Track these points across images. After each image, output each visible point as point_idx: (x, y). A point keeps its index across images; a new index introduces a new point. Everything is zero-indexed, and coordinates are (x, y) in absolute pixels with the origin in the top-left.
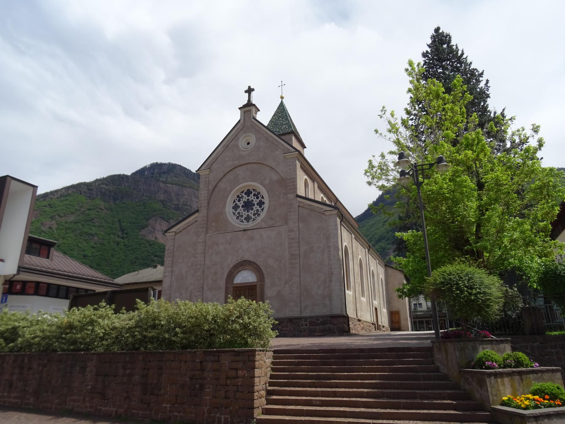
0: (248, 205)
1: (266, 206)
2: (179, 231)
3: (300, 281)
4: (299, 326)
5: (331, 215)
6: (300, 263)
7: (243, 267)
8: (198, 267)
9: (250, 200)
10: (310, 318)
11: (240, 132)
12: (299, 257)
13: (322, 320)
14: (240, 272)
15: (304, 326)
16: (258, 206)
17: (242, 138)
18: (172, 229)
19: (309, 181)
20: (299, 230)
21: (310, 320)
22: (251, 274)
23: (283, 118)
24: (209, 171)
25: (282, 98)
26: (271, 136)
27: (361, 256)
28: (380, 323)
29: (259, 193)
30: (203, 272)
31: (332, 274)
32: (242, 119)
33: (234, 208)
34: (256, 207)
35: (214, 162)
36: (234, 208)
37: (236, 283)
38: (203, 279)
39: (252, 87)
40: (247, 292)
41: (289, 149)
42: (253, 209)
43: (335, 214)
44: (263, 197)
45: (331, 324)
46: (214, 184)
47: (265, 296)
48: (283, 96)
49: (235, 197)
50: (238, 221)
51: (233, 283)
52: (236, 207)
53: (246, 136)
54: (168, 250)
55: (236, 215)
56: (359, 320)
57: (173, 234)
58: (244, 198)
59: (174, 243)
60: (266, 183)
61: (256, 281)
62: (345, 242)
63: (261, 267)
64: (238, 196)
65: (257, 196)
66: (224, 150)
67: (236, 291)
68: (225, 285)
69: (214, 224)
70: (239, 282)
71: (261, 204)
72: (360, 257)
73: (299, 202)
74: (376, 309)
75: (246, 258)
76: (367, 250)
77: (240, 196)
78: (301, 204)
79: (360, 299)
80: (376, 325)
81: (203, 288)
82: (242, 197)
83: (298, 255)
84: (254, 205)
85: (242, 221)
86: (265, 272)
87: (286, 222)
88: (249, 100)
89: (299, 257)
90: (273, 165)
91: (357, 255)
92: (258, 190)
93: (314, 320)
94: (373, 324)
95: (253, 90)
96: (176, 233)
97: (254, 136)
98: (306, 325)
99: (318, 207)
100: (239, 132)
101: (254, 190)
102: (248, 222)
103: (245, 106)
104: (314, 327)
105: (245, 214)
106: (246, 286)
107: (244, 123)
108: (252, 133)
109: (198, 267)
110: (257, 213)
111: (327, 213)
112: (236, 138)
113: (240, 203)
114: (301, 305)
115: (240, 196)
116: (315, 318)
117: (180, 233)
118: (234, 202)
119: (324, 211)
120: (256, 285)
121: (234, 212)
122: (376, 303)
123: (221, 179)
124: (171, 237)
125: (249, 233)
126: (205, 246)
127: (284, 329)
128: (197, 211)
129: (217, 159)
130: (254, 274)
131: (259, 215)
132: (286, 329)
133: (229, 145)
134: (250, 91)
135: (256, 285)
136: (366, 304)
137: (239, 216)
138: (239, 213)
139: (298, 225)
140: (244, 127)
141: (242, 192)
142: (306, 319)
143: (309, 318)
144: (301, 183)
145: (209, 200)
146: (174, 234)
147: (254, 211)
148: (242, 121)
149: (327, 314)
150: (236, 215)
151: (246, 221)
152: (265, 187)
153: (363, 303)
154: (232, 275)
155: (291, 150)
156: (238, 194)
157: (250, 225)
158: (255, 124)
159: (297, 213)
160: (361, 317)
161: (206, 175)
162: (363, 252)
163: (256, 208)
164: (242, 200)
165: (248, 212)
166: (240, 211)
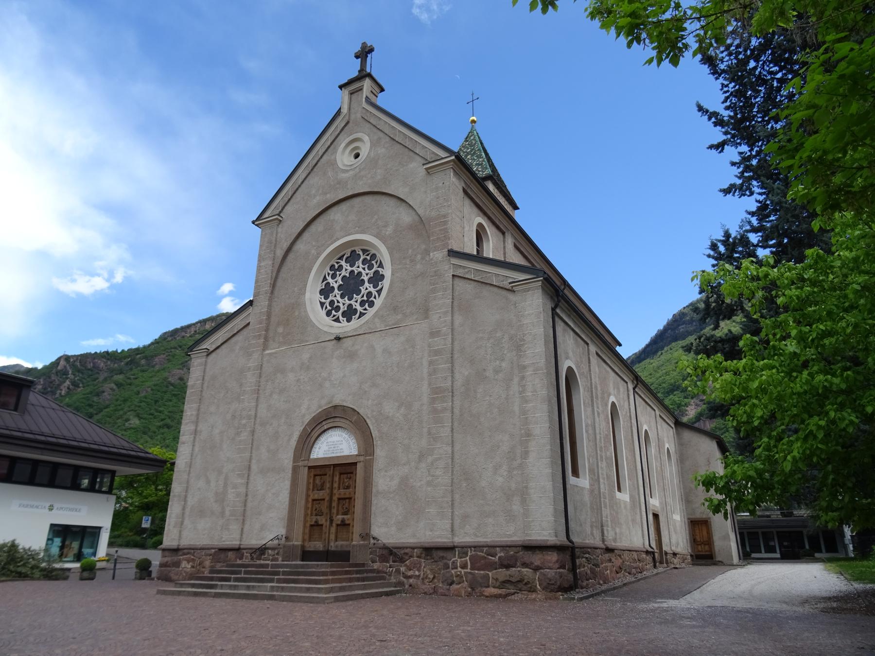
0: (351, 285)
1: (386, 284)
3: (453, 452)
4: (446, 567)
6: (452, 408)
7: (332, 420)
8: (244, 422)
9: (356, 272)
10: (475, 547)
11: (341, 135)
12: (453, 396)
13: (502, 554)
14: (325, 431)
15: (459, 569)
16: (371, 285)
18: (202, 343)
19: (490, 230)
20: (452, 330)
21: (473, 553)
22: (347, 436)
23: (472, 155)
24: (277, 219)
26: (400, 131)
27: (616, 398)
28: (665, 548)
29: (374, 256)
30: (253, 432)
31: (529, 434)
33: (322, 292)
34: (367, 287)
35: (289, 200)
36: (322, 292)
37: (315, 457)
38: (252, 448)
40: (337, 479)
41: (438, 155)
42: (360, 291)
44: (381, 265)
45: (525, 565)
46: (286, 245)
47: (374, 490)
50: (328, 320)
51: (308, 459)
52: (326, 291)
54: (193, 386)
55: (326, 308)
56: (609, 550)
59: (204, 372)
60: (387, 233)
62: (567, 358)
63: (368, 421)
64: (332, 267)
66: (309, 173)
67: (315, 476)
69: (280, 330)
70: (321, 455)
71: (377, 279)
72: (612, 399)
74: (656, 516)
75: (337, 401)
76: (631, 386)
77: (337, 266)
78: (460, 272)
79: (612, 497)
80: (656, 555)
81: (249, 468)
83: (450, 390)
85: (337, 320)
86: (375, 433)
87: (426, 313)
88: (362, 70)
89: (453, 396)
91: (603, 393)
92: (373, 251)
93: (483, 554)
94: (647, 552)
95: (371, 50)
96: (209, 353)
97: (367, 137)
98: (464, 566)
100: (339, 134)
101: (364, 251)
102: (349, 320)
104: (482, 572)
105: (344, 304)
106: (335, 466)
107: (349, 115)
108: (363, 132)
109: (244, 422)
110: (367, 301)
112: (332, 146)
113: (336, 282)
114: (452, 512)
115: (336, 267)
116: (485, 549)
117: (218, 351)
118: (325, 279)
119: (510, 283)
121: (323, 300)
122: (655, 503)
126: (260, 377)
127: (410, 573)
131: (371, 304)
132: (417, 573)
133: (319, 164)
134: (365, 53)
135: (355, 464)
136: (628, 507)
138: (332, 303)
139: (452, 319)
140: (348, 123)
142: (464, 549)
143: (470, 547)
144: (467, 229)
146: (205, 354)
147: (363, 297)
149: (515, 538)
150: (326, 308)
151: (345, 319)
153: (623, 506)
154: (308, 439)
157: (355, 323)
159: (450, 291)
160: (615, 540)
162: (621, 390)
163: (367, 289)
164: (340, 275)
165: (350, 299)
166: (334, 299)
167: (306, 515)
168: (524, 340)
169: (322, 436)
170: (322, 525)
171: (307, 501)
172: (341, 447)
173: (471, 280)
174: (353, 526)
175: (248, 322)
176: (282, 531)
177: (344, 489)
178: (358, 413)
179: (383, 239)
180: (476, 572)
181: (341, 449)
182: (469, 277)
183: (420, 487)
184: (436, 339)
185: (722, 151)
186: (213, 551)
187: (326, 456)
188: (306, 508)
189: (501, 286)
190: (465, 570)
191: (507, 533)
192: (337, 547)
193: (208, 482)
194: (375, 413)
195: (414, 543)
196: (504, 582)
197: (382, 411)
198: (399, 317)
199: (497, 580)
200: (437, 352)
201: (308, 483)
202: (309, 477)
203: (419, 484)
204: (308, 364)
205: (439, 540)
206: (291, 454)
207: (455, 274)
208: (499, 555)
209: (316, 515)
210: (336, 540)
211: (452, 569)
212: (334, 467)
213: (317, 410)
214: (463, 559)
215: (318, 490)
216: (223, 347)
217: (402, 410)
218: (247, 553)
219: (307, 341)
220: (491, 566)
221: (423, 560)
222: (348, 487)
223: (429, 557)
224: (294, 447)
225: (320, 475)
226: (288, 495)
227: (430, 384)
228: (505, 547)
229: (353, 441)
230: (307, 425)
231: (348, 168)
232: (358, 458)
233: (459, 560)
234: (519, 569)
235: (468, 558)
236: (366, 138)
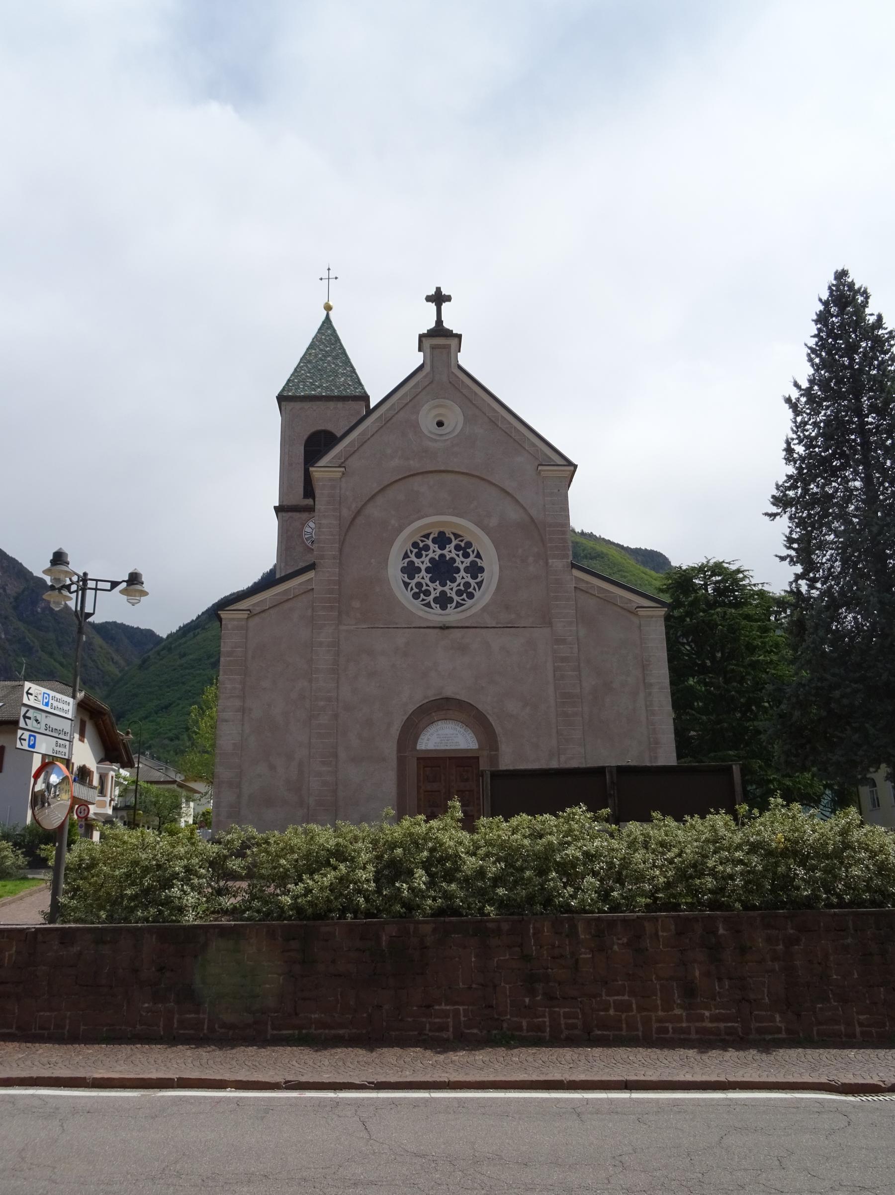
2: (258, 609)
5: (652, 617)
17: (426, 407)
18: (240, 603)
20: (578, 639)
22: (462, 730)
23: (335, 358)
25: (328, 308)
26: (502, 417)
29: (469, 545)
30: (336, 716)
32: (428, 362)
37: (423, 748)
39: (445, 292)
41: (550, 458)
43: (660, 616)
48: (331, 303)
49: (409, 546)
53: (437, 406)
57: (245, 615)
58: (431, 551)
63: (488, 717)
64: (415, 545)
65: (464, 549)
66: (382, 427)
67: (425, 767)
70: (431, 746)
73: (578, 579)
75: (450, 691)
78: (583, 586)
81: (336, 755)
82: (427, 548)
84: (458, 570)
86: (498, 730)
88: (439, 321)
90: (509, 486)
92: (468, 538)
95: (448, 298)
99: (621, 597)
100: (420, 392)
101: (457, 536)
103: (431, 334)
105: (435, 589)
106: (450, 758)
109: (322, 703)
111: (642, 612)
113: (423, 563)
117: (263, 615)
120: (478, 758)
123: (372, 498)
124: (236, 623)
125: (457, 634)
128: (312, 567)
129: (362, 445)
130: (470, 731)
134: (439, 298)
135: (478, 758)
137: (420, 592)
141: (427, 536)
145: (342, 543)
146: (246, 616)
148: (427, 368)
152: (487, 534)
155: (553, 461)
156: (416, 538)
157: (451, 615)
158: (463, 382)
161: (331, 480)
163: (463, 578)
173: (595, 595)
175: (310, 587)
178: (477, 709)
179: (484, 528)
181: (457, 742)
182: (592, 593)
184: (562, 647)
185: (773, 520)
187: (438, 748)
189: (625, 607)
193: (272, 768)
198: (513, 616)
207: (578, 586)
216: (271, 611)
219: (397, 624)
229: (470, 735)
231: (438, 438)
236: (457, 409)
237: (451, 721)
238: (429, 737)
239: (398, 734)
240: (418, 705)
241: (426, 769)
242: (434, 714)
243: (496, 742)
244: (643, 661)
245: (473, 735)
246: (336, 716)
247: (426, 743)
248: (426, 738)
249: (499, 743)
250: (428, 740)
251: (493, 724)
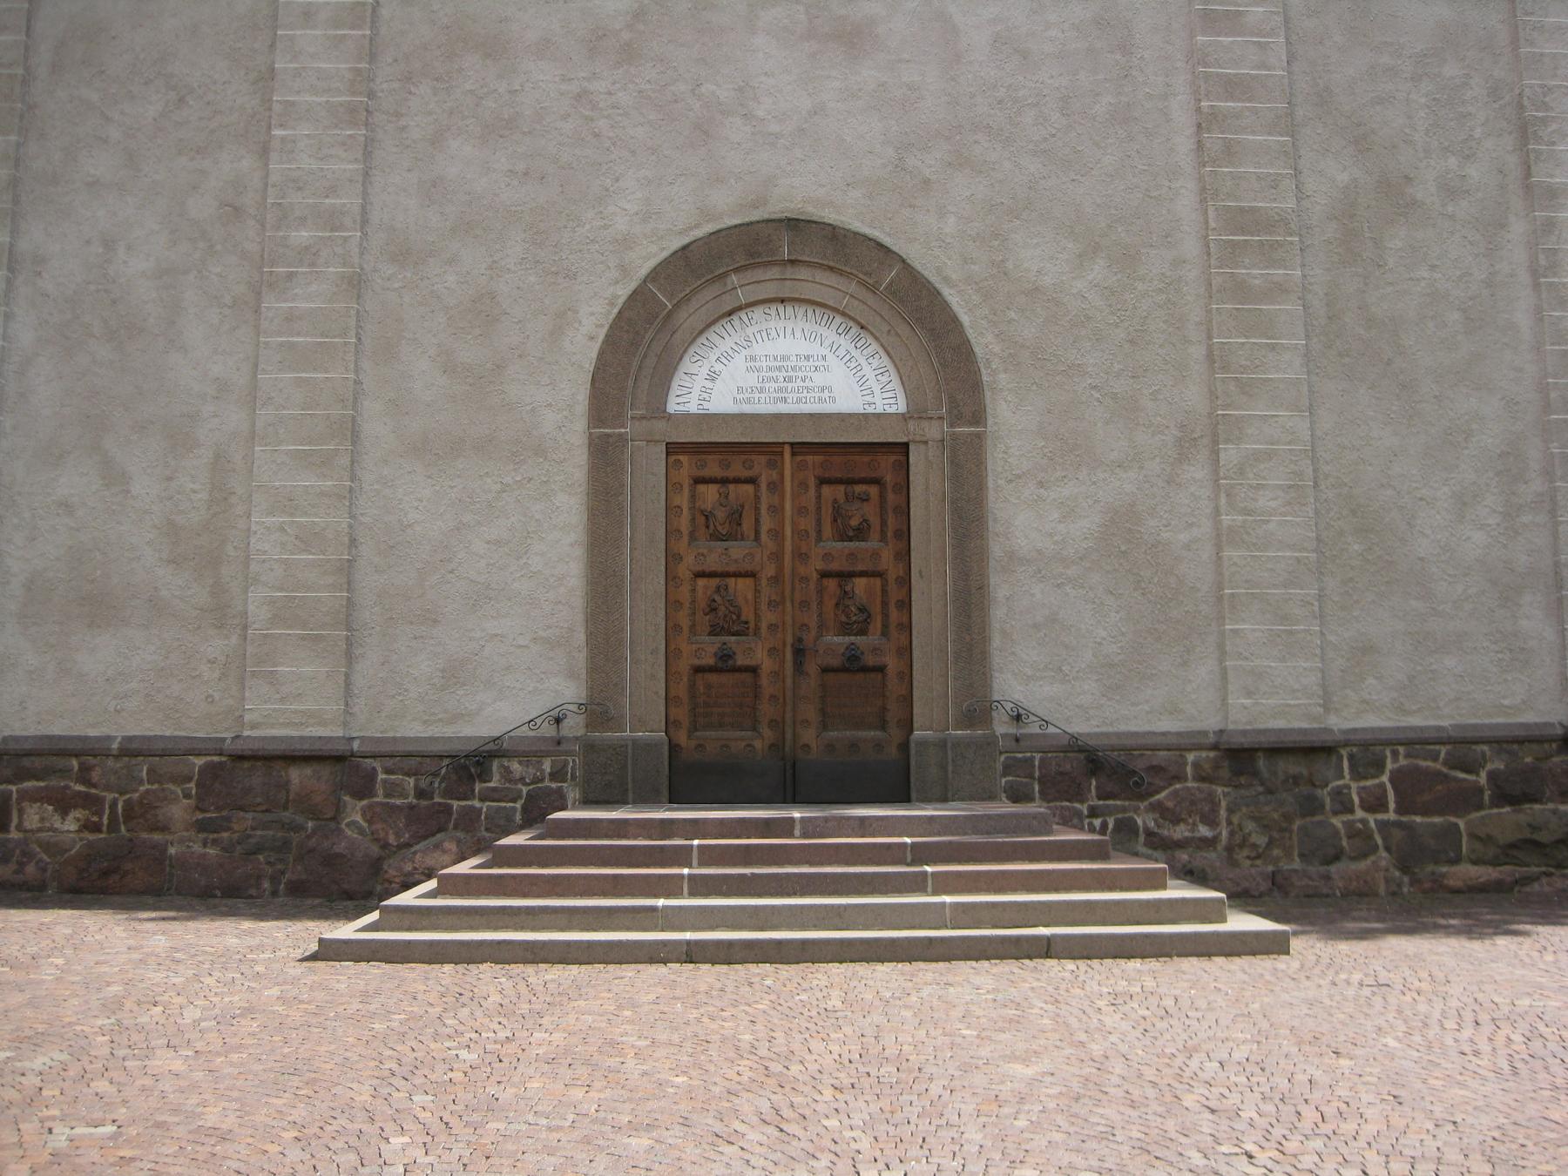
4: (1311, 806)
7: (774, 272)
15: (1360, 814)
20: (1287, 21)
21: (1403, 762)
22: (845, 343)
30: (356, 284)
37: (693, 408)
47: (996, 550)
51: (658, 410)
61: (900, 406)
63: (946, 292)
68: (580, 425)
70: (722, 400)
81: (352, 432)
86: (983, 342)
93: (1438, 766)
98: (1375, 803)
104: (1437, 820)
106: (799, 448)
109: (303, 235)
126: (372, 57)
127: (1180, 832)
132: (1204, 831)
149: (1530, 718)
167: (672, 629)
168: (1546, 107)
169: (717, 328)
170: (753, 670)
171: (671, 577)
172: (819, 379)
174: (907, 676)
176: (566, 690)
177: (843, 537)
178: (904, 261)
180: (1418, 819)
183: (1187, 547)
186: (199, 762)
187: (747, 409)
188: (672, 604)
190: (1380, 816)
191: (1506, 702)
192: (830, 747)
194: (976, 268)
195: (1179, 734)
196: (1513, 846)
197: (1009, 264)
199: (1488, 840)
200: (1233, 87)
201: (671, 510)
202: (672, 487)
203: (1183, 537)
204: (626, 36)
205: (1280, 724)
206: (574, 390)
208: (1489, 767)
209: (715, 631)
210: (824, 726)
211: (1335, 813)
212: (793, 454)
213: (697, 226)
214: (1369, 783)
215: (716, 537)
217: (1098, 270)
218: (388, 771)
220: (1466, 800)
221: (1219, 790)
222: (860, 533)
223: (1243, 780)
224: (589, 366)
225: (724, 481)
226: (580, 552)
227: (1205, 193)
228: (1510, 741)
230: (654, 275)
232: (911, 425)
233: (1354, 785)
234: (1551, 806)
235: (1385, 778)
237: (800, 311)
238: (718, 367)
239: (594, 355)
240: (676, 244)
241: (702, 488)
242: (734, 277)
243: (976, 387)
244: (1521, 107)
245: (886, 361)
246: (356, 284)
247: (705, 390)
248: (704, 371)
249: (988, 394)
250: (713, 377)
251: (965, 319)
